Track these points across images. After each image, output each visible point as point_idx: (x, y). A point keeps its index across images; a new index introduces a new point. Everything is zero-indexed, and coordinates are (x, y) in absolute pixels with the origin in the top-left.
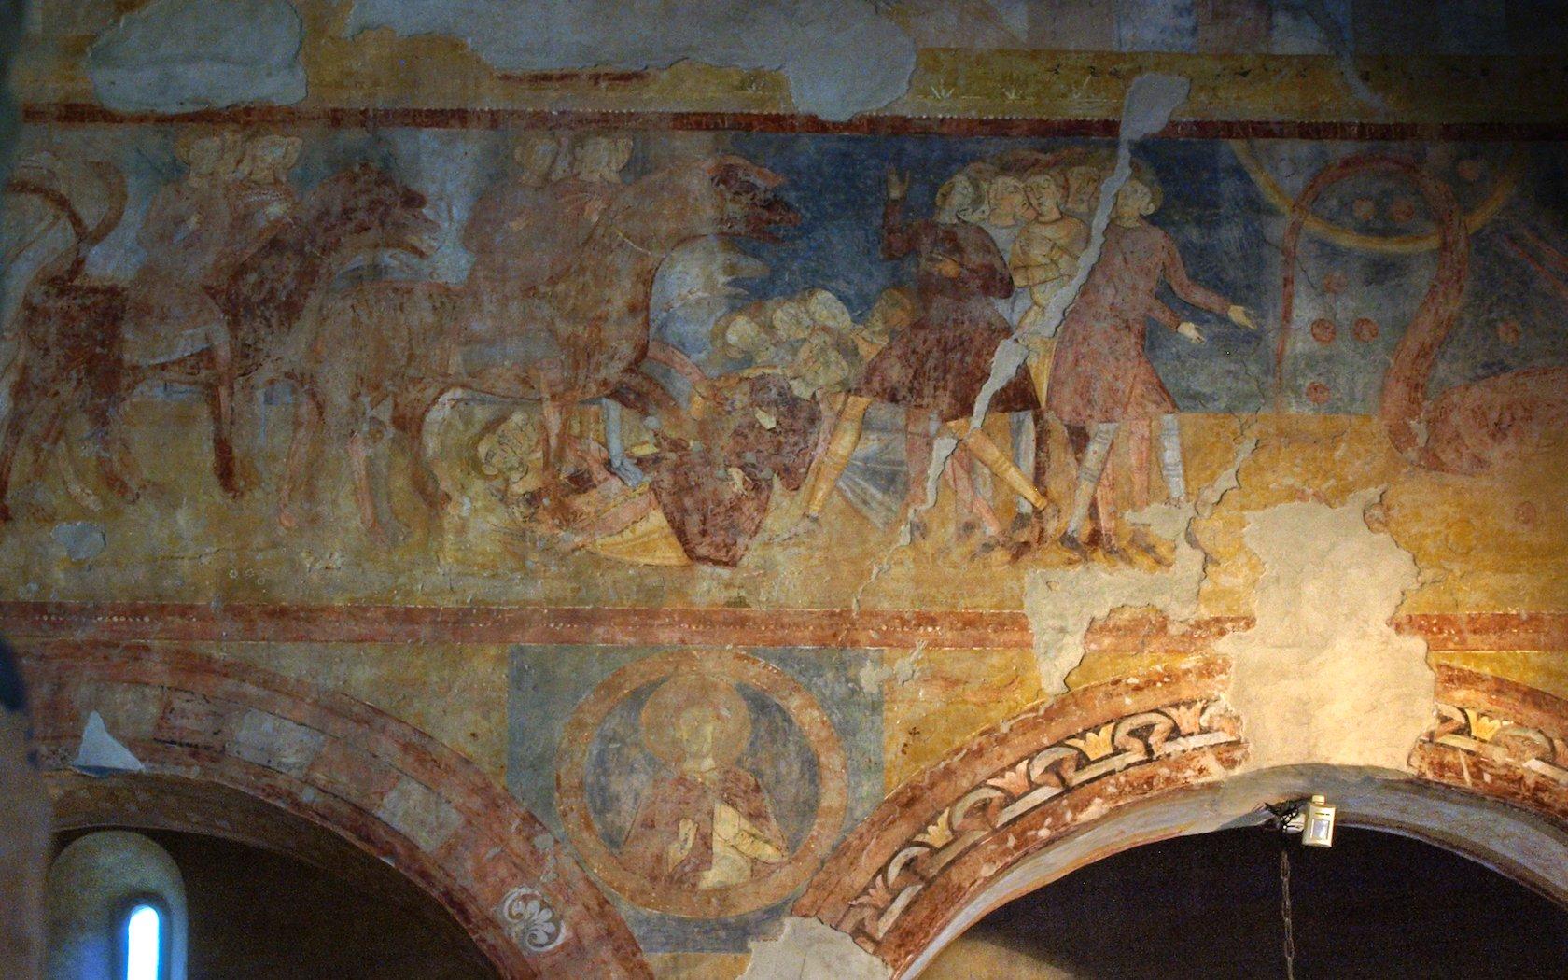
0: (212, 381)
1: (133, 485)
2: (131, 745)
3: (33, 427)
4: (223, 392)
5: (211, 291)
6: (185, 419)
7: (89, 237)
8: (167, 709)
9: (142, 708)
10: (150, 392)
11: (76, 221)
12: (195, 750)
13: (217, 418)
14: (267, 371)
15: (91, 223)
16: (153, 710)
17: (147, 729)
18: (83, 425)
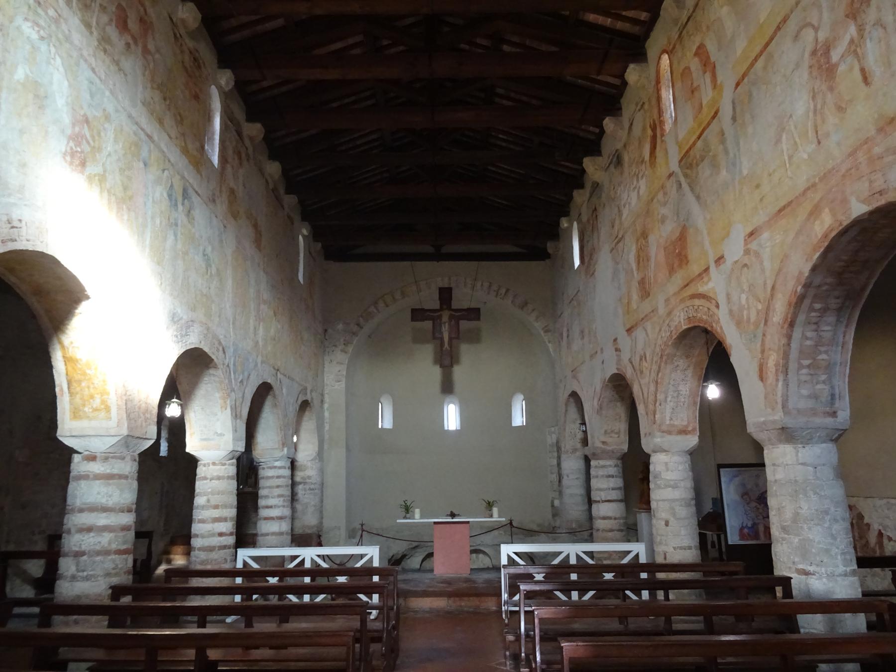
0: (855, 49)
1: (844, 106)
2: (863, 202)
3: (819, 106)
4: (858, 50)
5: (847, 16)
6: (851, 69)
7: (816, 29)
8: (871, 182)
9: (863, 187)
10: (842, 68)
11: (813, 26)
12: (881, 193)
13: (859, 61)
14: (868, 28)
15: (816, 25)
16: (867, 184)
17: (867, 194)
18: (829, 95)
